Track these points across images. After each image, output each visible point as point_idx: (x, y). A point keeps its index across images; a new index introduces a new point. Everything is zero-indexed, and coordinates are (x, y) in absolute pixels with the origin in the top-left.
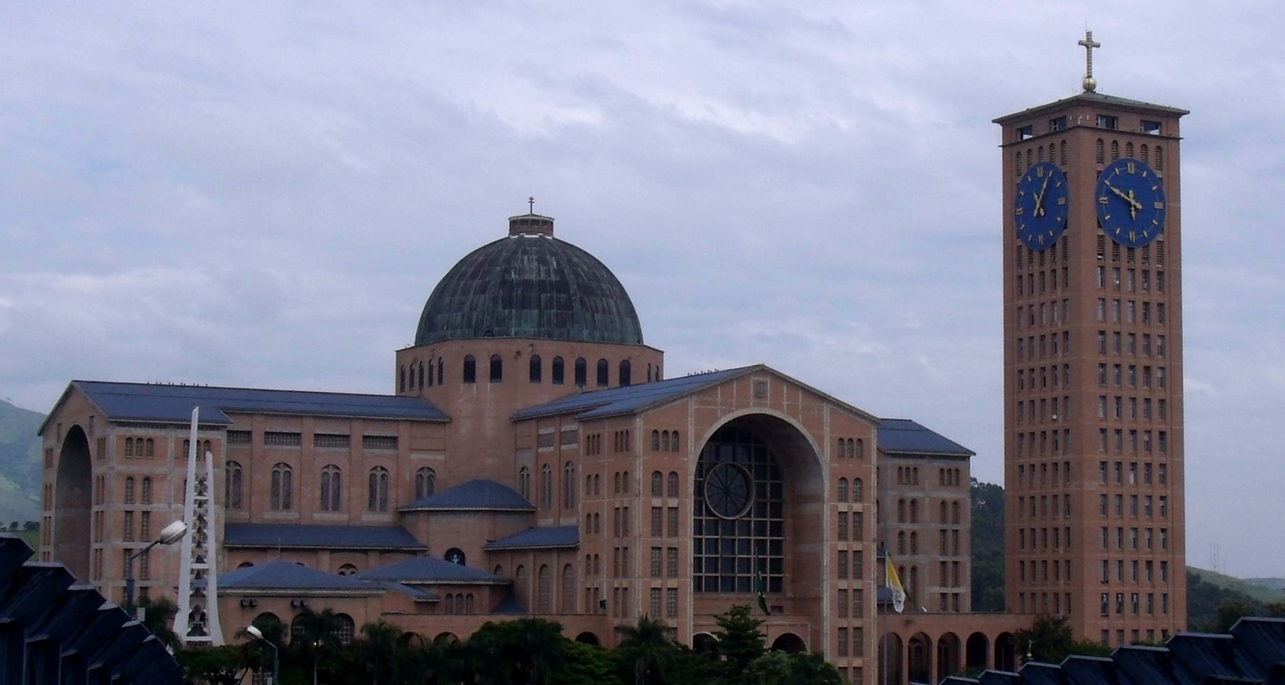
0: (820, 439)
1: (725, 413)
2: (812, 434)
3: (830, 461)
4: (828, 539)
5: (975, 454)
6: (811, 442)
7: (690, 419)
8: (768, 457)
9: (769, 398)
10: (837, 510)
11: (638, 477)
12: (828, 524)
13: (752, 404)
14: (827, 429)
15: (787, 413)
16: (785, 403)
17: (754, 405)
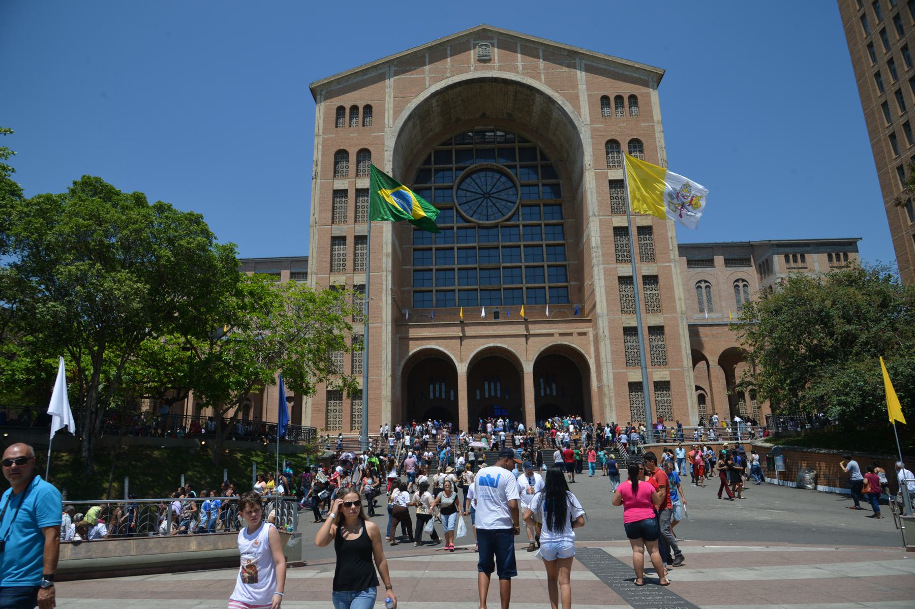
0: (574, 100)
1: (435, 80)
2: (563, 95)
3: (591, 120)
4: (596, 213)
5: (861, 239)
6: (560, 102)
7: (387, 90)
8: (539, 157)
9: (496, 61)
10: (607, 177)
11: (315, 159)
12: (595, 196)
13: (472, 68)
14: (582, 87)
15: (523, 74)
16: (520, 65)
17: (476, 70)
